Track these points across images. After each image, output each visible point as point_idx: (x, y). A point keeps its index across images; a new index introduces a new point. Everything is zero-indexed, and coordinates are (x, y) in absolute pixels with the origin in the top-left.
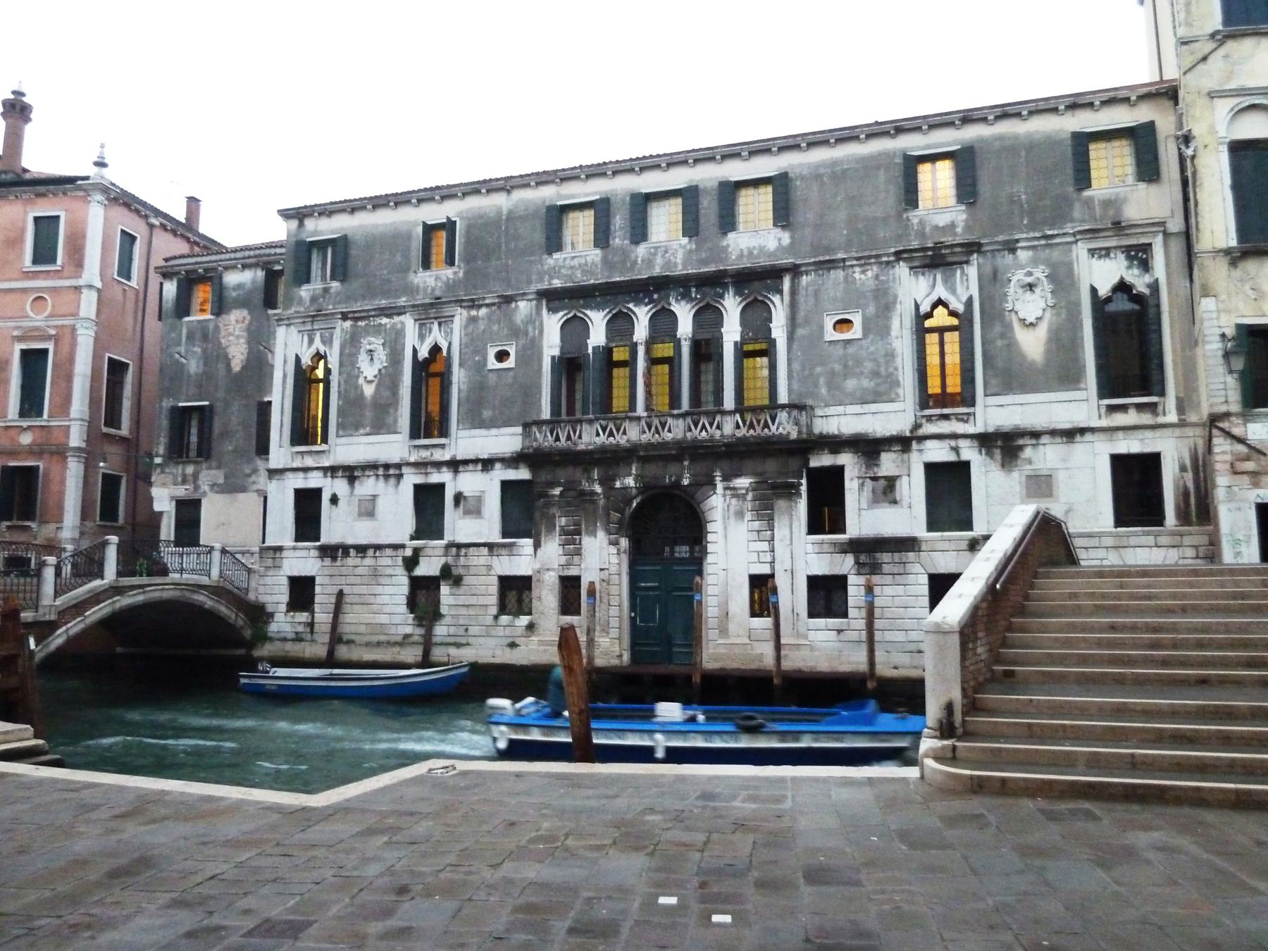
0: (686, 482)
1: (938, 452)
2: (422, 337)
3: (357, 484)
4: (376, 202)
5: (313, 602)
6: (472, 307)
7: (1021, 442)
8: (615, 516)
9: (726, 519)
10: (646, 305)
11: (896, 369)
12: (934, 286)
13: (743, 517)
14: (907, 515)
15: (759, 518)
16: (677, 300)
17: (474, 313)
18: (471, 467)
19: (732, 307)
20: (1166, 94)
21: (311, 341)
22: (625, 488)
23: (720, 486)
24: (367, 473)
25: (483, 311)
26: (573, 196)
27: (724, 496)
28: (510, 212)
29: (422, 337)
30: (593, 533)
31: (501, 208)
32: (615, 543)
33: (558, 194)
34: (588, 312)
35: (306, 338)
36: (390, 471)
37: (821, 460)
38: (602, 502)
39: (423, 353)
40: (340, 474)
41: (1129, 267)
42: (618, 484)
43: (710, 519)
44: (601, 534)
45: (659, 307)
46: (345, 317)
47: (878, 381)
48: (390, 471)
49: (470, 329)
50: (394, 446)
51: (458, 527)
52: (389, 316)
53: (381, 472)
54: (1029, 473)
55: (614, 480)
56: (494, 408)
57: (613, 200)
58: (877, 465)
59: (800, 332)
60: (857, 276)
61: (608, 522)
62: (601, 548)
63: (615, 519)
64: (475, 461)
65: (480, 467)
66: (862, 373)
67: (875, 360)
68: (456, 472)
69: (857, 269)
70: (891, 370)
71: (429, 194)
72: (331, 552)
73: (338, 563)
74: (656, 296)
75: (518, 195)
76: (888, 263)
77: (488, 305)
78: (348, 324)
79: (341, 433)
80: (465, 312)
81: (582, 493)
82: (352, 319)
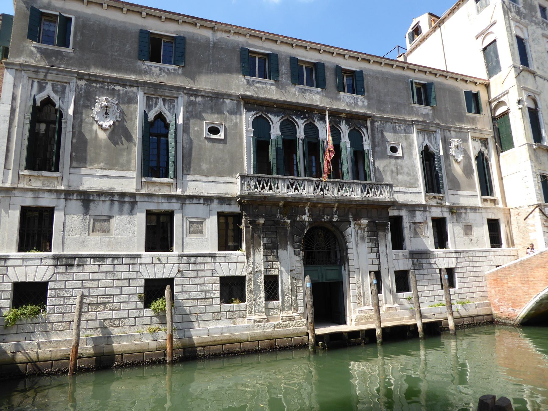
0: (335, 219)
1: (437, 213)
2: (149, 107)
3: (92, 205)
4: (150, 12)
5: (45, 303)
6: (192, 95)
7: (461, 211)
8: (296, 238)
9: (357, 241)
10: (302, 119)
11: (417, 173)
12: (424, 139)
13: (364, 240)
14: (428, 240)
15: (371, 241)
16: (318, 120)
17: (192, 99)
18: (195, 201)
19: (345, 129)
20: (485, 85)
21: (41, 89)
22: (302, 222)
23: (352, 225)
24: (103, 198)
25: (199, 99)
26: (306, 58)
27: (354, 228)
28: (215, 44)
29: (149, 107)
30: (285, 248)
31: (209, 38)
32: (297, 254)
33: (247, 42)
34: (272, 117)
35: (36, 85)
36: (126, 201)
37: (393, 213)
38: (289, 229)
39: (151, 116)
40: (75, 197)
41: (482, 146)
42: (298, 219)
43: (348, 240)
44: (290, 248)
45: (309, 122)
46: (80, 77)
47: (410, 177)
48: (126, 201)
49: (190, 108)
50: (128, 181)
51: (185, 242)
52: (124, 86)
53: (116, 198)
54: (465, 224)
55: (297, 216)
56: (210, 163)
57: (280, 56)
58: (415, 217)
59: (377, 149)
60: (397, 127)
61: (293, 242)
62: (291, 257)
63: (297, 239)
64: (198, 197)
65: (202, 201)
66: (404, 173)
67: (408, 168)
68: (183, 203)
69: (397, 124)
70: (415, 173)
71: (158, 14)
72: (66, 261)
73: (75, 269)
74: (307, 115)
75: (220, 35)
76: (408, 124)
77: (202, 96)
78: (82, 83)
79: (74, 164)
80: (186, 97)
81: (277, 223)
82: (86, 80)
